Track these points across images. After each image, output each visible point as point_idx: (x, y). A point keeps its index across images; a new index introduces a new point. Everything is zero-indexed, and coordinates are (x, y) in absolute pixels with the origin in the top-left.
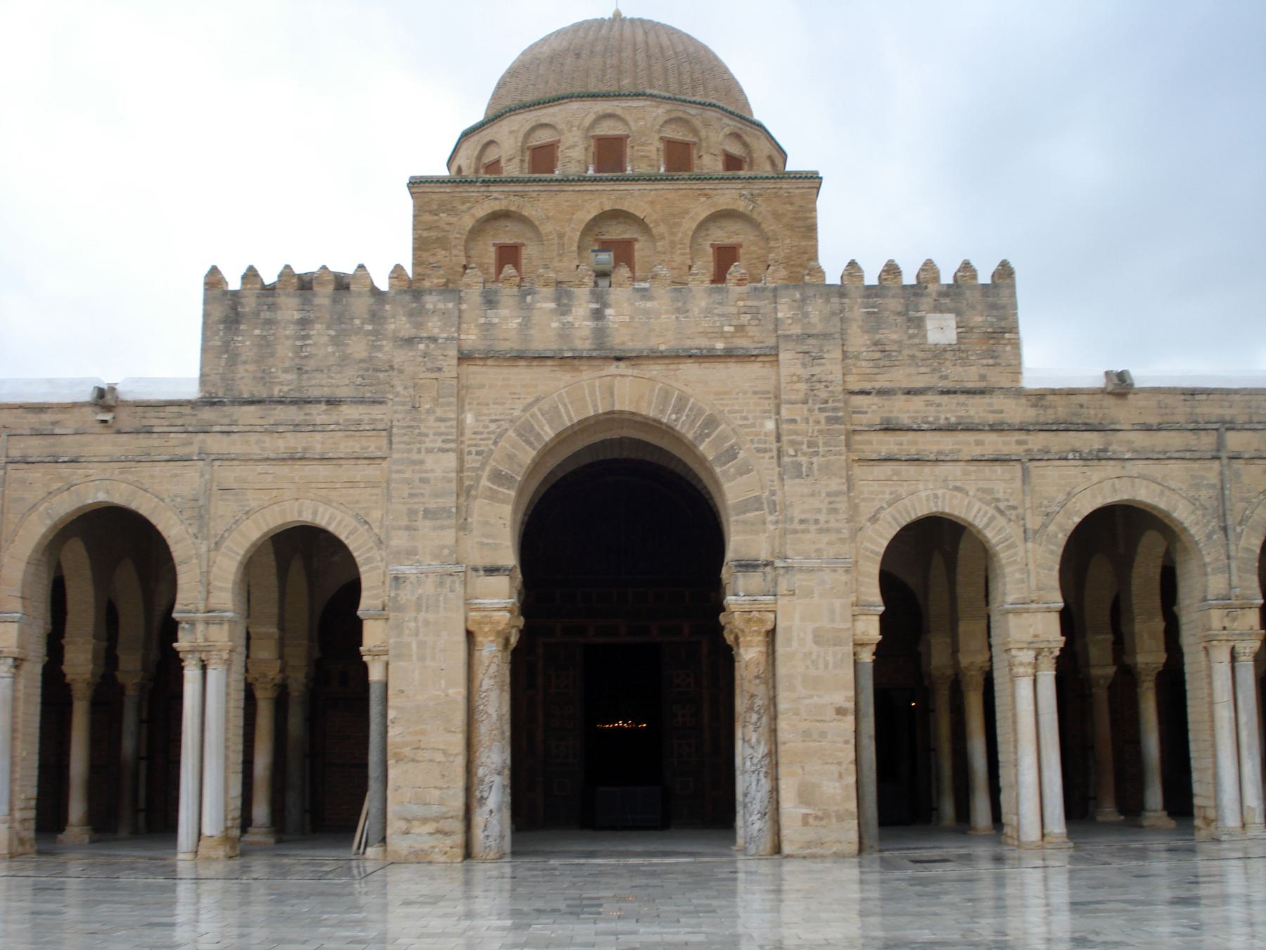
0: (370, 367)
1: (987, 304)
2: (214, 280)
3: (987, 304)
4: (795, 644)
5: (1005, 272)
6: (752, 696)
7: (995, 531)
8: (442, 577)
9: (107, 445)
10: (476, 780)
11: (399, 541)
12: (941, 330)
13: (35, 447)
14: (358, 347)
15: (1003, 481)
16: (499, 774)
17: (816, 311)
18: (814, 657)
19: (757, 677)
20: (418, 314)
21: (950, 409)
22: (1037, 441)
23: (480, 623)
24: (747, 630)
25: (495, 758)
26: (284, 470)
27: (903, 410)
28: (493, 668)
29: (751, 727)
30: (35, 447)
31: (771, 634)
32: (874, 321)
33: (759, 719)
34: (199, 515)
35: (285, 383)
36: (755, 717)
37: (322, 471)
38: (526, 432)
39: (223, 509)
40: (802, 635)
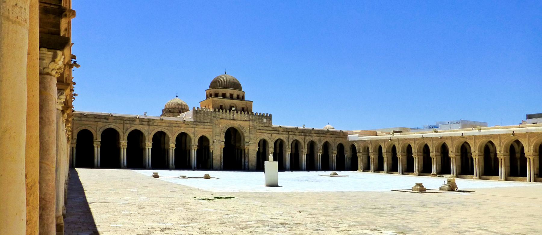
0: (211, 119)
1: (269, 117)
2: (194, 108)
3: (269, 117)
5: (271, 115)
7: (269, 141)
8: (219, 142)
9: (184, 125)
11: (214, 138)
12: (265, 120)
13: (176, 125)
14: (209, 117)
15: (269, 136)
17: (254, 117)
20: (216, 114)
21: (265, 128)
22: (273, 132)
25: (222, 160)
26: (202, 130)
27: (261, 128)
30: (176, 125)
31: (248, 150)
32: (259, 119)
34: (194, 134)
35: (202, 120)
37: (206, 130)
38: (226, 127)
39: (196, 133)
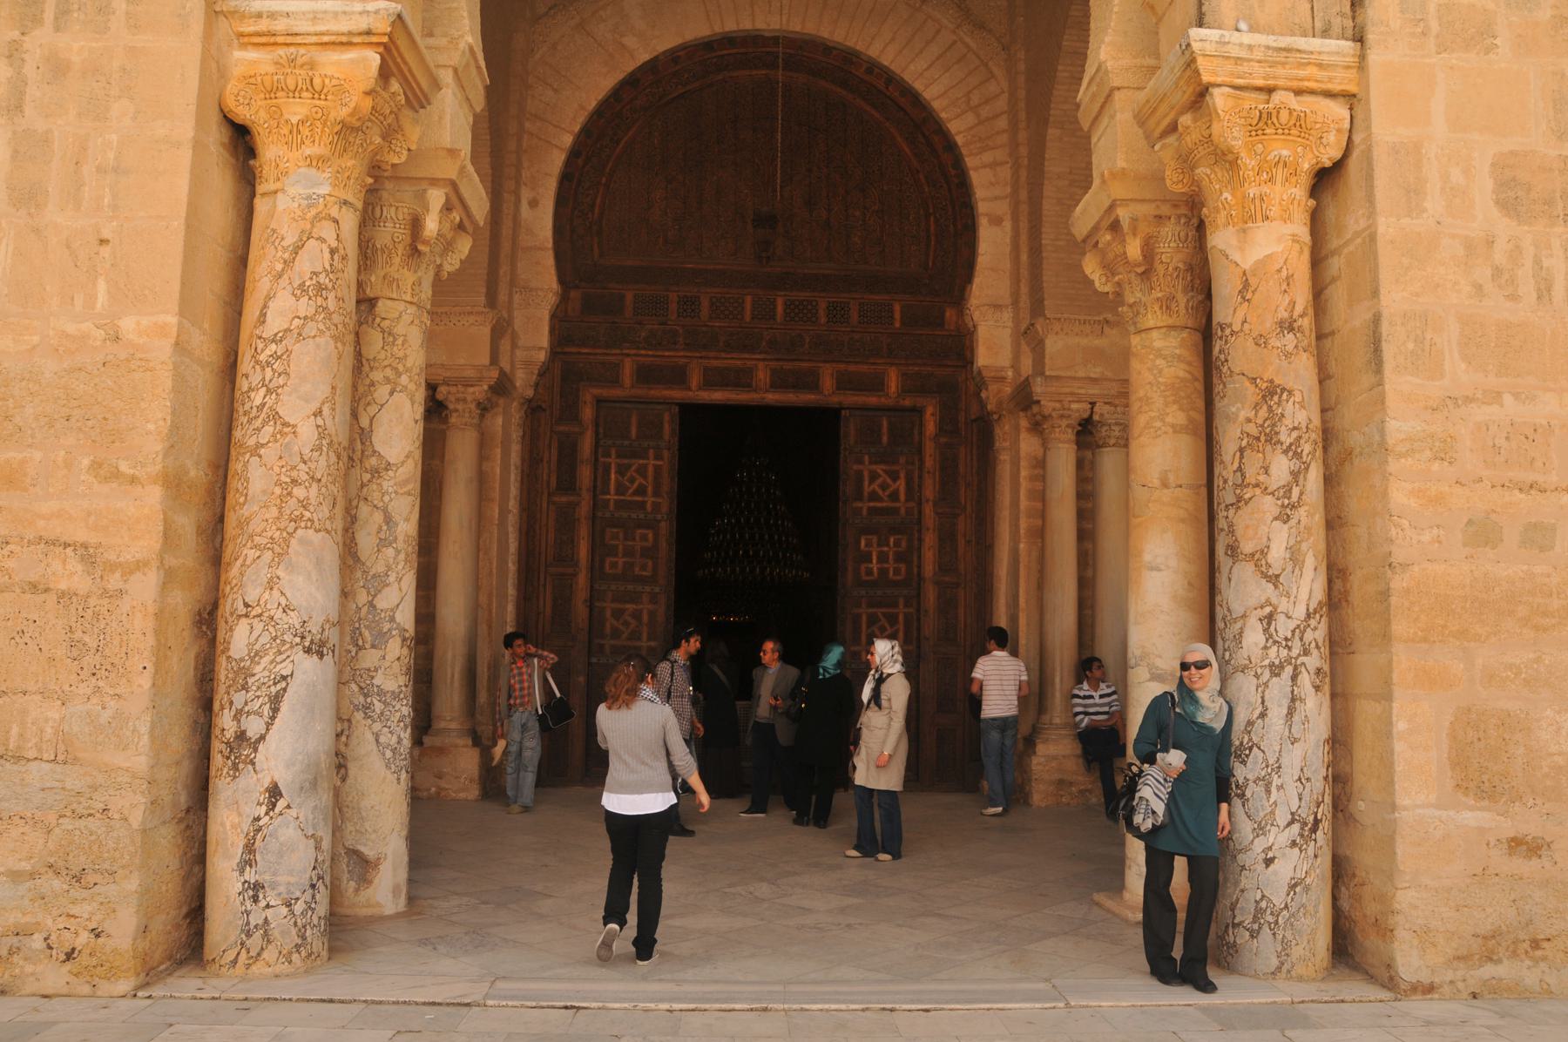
4: (1434, 204)
6: (1272, 392)
10: (223, 672)
16: (316, 649)
18: (1499, 257)
19: (1288, 326)
23: (271, 92)
24: (1248, 162)
28: (313, 259)
29: (1269, 505)
33: (1295, 475)
36: (1281, 467)
40: (1456, 176)
